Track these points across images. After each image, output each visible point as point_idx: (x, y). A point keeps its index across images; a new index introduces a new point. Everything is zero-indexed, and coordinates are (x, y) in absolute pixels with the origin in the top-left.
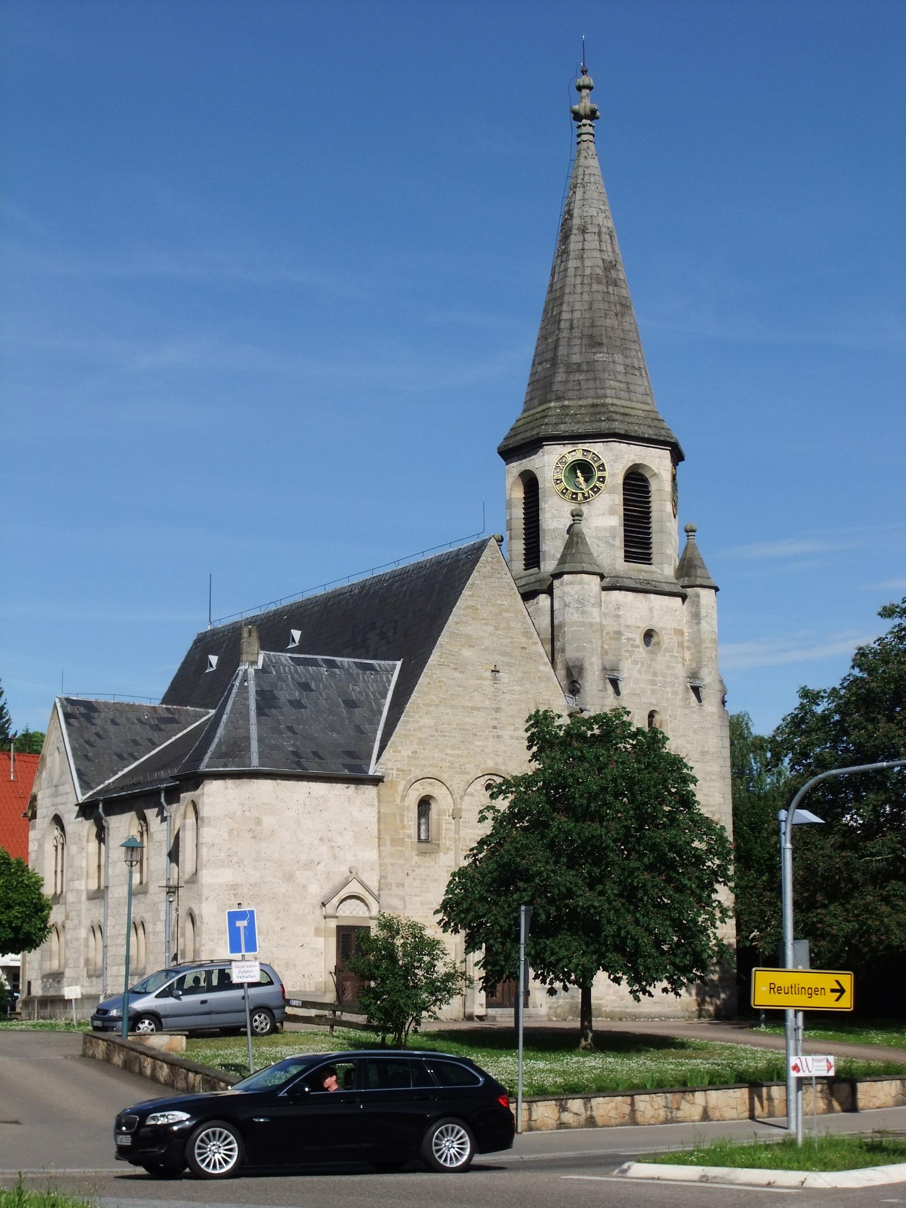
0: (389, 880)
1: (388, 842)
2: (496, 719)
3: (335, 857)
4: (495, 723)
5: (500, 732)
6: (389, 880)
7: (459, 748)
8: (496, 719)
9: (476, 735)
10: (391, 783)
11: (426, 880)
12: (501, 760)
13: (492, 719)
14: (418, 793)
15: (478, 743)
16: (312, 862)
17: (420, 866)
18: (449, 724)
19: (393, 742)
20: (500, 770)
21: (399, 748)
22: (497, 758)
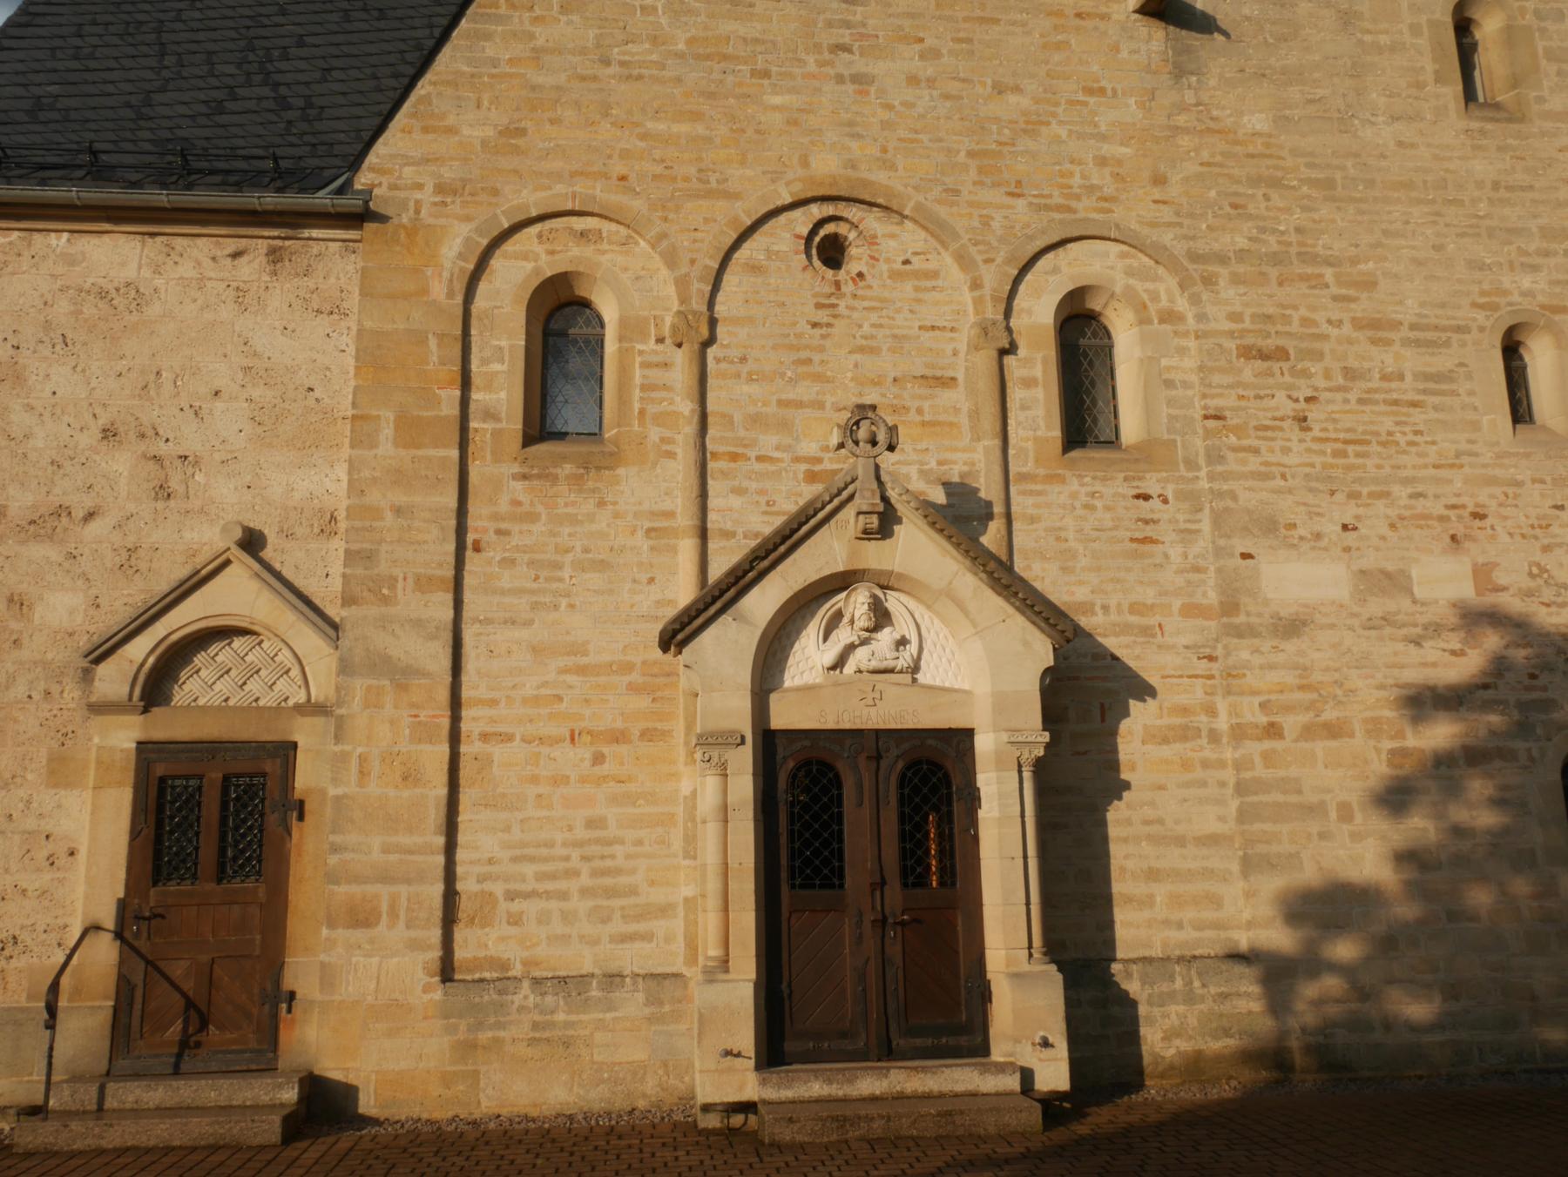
0: (383, 568)
1: (387, 432)
2: (847, 24)
3: (163, 492)
4: (845, 36)
5: (860, 65)
6: (383, 568)
7: (696, 116)
8: (847, 24)
9: (766, 74)
10: (412, 232)
11: (558, 566)
12: (874, 151)
13: (830, 24)
14: (529, 266)
15: (777, 100)
16: (62, 511)
17: (532, 517)
18: (654, 40)
19: (426, 99)
20: (866, 184)
21: (451, 120)
22: (854, 145)
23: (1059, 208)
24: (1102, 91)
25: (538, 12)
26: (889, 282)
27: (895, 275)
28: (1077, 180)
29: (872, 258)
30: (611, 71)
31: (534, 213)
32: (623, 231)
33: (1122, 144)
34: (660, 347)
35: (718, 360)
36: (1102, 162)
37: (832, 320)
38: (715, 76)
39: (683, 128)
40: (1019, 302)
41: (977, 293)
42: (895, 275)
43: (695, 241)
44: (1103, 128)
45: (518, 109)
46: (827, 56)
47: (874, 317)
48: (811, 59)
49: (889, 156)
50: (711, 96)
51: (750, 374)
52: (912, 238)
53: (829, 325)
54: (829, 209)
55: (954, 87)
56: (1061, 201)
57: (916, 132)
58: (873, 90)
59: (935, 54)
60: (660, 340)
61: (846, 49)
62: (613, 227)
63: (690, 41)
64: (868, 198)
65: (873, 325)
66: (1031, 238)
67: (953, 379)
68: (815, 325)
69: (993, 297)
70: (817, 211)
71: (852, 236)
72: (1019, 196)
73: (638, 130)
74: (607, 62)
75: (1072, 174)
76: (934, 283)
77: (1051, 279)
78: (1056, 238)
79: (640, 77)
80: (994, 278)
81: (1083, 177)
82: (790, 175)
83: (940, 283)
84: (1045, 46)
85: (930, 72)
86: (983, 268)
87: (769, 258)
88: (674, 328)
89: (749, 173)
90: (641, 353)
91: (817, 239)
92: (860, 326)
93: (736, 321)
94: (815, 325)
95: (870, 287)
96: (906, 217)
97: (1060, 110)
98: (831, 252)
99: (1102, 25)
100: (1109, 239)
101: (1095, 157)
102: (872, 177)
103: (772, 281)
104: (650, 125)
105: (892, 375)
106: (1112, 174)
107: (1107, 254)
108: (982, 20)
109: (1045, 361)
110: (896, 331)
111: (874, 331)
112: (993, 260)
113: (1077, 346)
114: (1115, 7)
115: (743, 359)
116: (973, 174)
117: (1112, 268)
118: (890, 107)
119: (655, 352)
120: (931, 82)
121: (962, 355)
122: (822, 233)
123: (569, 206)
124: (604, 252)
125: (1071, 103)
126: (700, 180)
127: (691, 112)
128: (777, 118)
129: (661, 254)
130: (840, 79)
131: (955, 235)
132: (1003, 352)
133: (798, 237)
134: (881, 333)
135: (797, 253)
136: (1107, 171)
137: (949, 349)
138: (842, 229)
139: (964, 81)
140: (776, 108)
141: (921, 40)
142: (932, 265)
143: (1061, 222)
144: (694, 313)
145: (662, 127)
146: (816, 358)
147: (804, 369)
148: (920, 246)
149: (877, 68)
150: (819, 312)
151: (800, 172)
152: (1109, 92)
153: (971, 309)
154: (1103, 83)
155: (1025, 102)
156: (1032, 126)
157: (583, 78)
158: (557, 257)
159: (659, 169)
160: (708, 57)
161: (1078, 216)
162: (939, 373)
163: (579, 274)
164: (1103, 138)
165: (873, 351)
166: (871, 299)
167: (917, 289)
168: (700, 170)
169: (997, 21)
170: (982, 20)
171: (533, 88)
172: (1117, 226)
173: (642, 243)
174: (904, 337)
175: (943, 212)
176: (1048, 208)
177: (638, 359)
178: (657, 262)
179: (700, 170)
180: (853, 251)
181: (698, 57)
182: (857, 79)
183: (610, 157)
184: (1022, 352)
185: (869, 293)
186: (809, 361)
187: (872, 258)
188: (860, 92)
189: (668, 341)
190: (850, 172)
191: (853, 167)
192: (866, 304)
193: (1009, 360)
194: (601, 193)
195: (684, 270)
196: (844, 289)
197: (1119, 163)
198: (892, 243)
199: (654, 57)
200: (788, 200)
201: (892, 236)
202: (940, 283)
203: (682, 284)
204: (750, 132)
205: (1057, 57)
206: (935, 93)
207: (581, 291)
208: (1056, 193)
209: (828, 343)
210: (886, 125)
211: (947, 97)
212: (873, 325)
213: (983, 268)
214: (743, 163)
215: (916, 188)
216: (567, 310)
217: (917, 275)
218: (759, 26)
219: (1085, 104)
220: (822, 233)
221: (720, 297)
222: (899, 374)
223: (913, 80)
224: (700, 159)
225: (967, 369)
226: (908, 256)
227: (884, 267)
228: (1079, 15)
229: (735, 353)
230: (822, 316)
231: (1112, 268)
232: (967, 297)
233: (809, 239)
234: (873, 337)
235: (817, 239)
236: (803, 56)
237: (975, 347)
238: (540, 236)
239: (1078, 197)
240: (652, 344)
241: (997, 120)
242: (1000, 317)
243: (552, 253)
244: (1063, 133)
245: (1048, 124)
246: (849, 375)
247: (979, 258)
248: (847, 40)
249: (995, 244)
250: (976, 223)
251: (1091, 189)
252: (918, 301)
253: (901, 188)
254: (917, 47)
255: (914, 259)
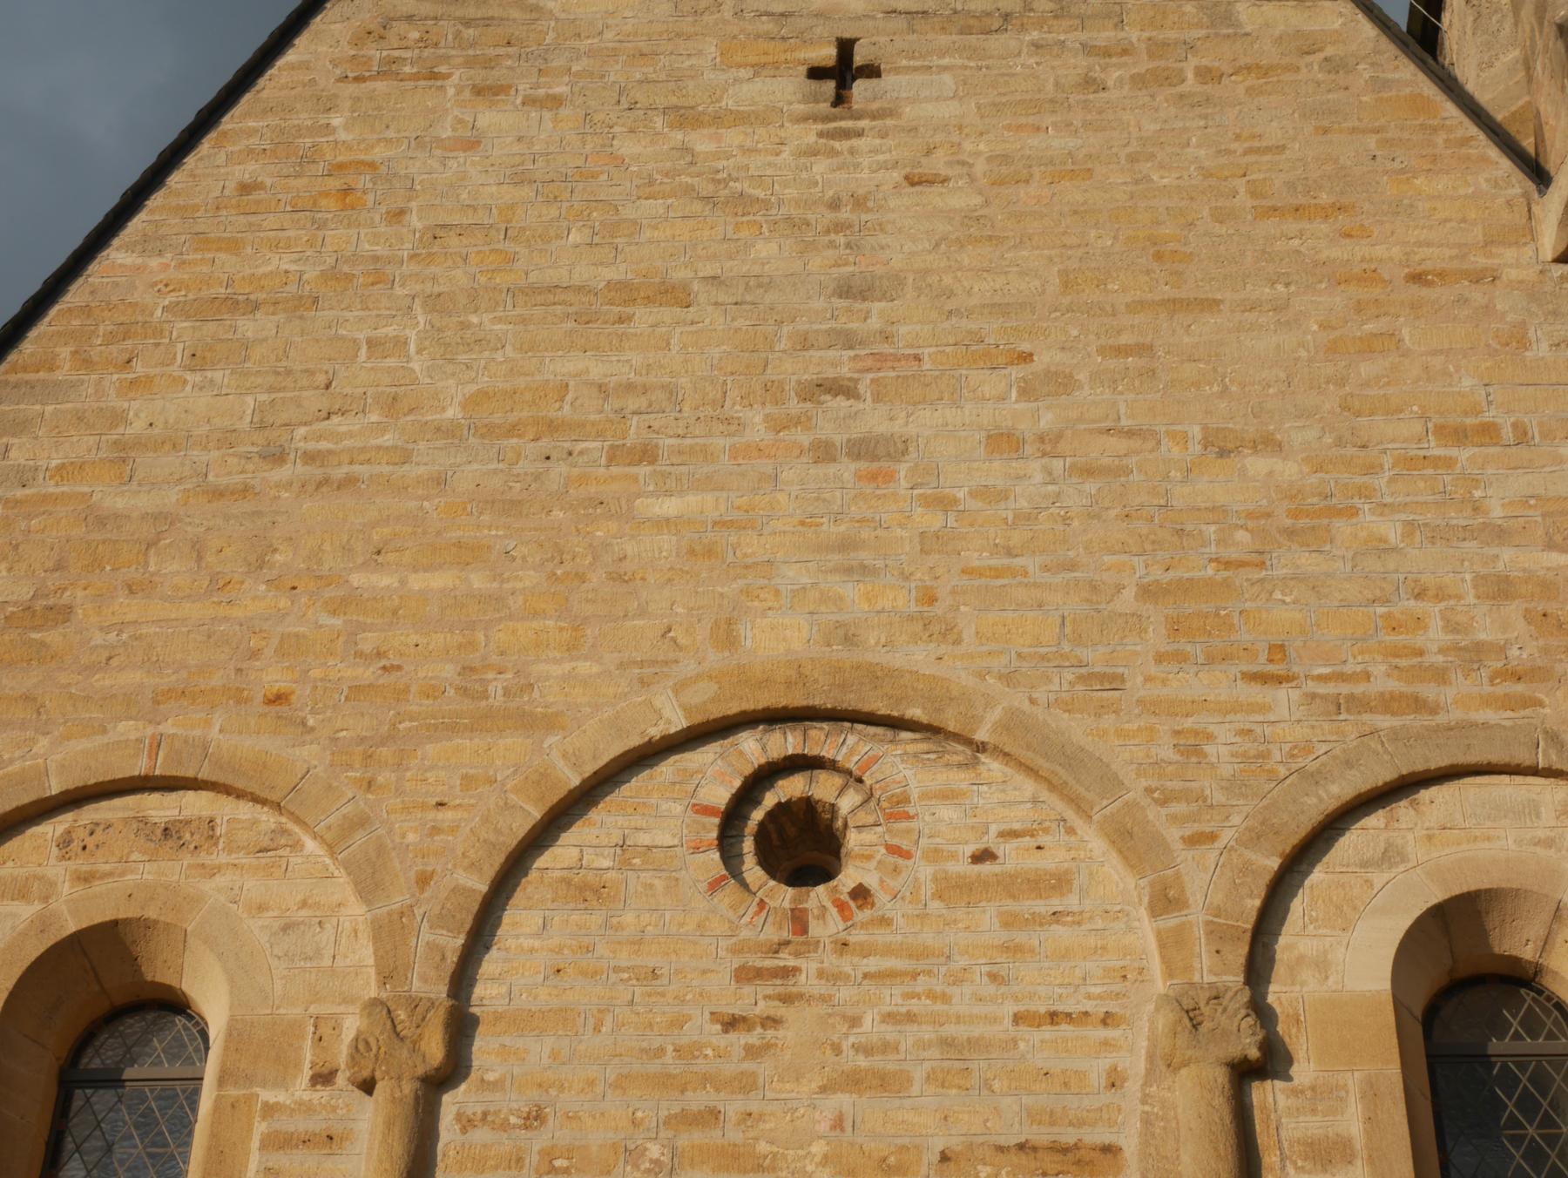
2: (848, 340)
4: (841, 363)
5: (874, 419)
7: (467, 554)
8: (848, 340)
9: (647, 454)
12: (901, 600)
14: (27, 911)
15: (669, 507)
18: (392, 405)
20: (876, 676)
22: (851, 591)
23: (1388, 703)
24: (1488, 432)
25: (139, 368)
26: (935, 905)
27: (950, 889)
28: (1435, 636)
29: (893, 850)
30: (284, 473)
31: (55, 787)
32: (267, 819)
33: (1550, 546)
34: (322, 1094)
35: (466, 1123)
36: (1499, 589)
37: (779, 1010)
38: (523, 467)
39: (440, 580)
40: (1291, 942)
41: (1170, 921)
42: (950, 889)
43: (436, 830)
44: (1497, 512)
45: (59, 566)
46: (794, 406)
47: (892, 997)
48: (756, 417)
49: (938, 609)
50: (512, 507)
51: (548, 1155)
52: (1000, 797)
53: (771, 1022)
54: (785, 742)
55: (1105, 450)
56: (1394, 685)
57: (1009, 553)
58: (903, 469)
59: (1061, 382)
60: (323, 1078)
61: (845, 389)
62: (245, 810)
63: (471, 403)
64: (882, 709)
65: (889, 1018)
66: (1315, 778)
67: (1109, 1150)
68: (732, 1023)
69: (1213, 931)
70: (754, 748)
71: (847, 803)
72: (1279, 680)
73: (329, 593)
74: (277, 457)
75: (1420, 622)
76: (1056, 904)
77: (1379, 878)
78: (1382, 774)
79: (349, 482)
80: (1221, 885)
81: (1451, 626)
82: (688, 667)
83: (1072, 902)
84: (1333, 349)
85: (1047, 421)
86: (1186, 859)
87: (624, 864)
88: (360, 1045)
89: (585, 667)
90: (269, 1110)
91: (758, 815)
92: (855, 1022)
93: (524, 1022)
94: (732, 1023)
95: (885, 921)
96: (981, 748)
97: (1381, 481)
98: (802, 848)
99: (1477, 296)
100: (1534, 771)
101: (1479, 580)
102: (897, 660)
103: (629, 918)
104: (357, 579)
105: (939, 1144)
106: (1528, 616)
107: (1533, 810)
108: (1175, 306)
109: (1371, 1093)
110: (950, 1030)
111: (890, 1032)
112: (1212, 837)
113: (1485, 1060)
114: (1510, 254)
115: (535, 1118)
116: (1156, 637)
117: (1549, 843)
118: (944, 503)
119: (307, 1108)
120: (1048, 444)
121: (1133, 1087)
122: (770, 800)
123: (140, 767)
124: (213, 872)
125: (1409, 463)
126: (464, 691)
127: (459, 545)
128: (667, 541)
129: (347, 866)
130: (824, 452)
131: (1111, 783)
132: (1245, 1073)
133: (706, 810)
134: (909, 1036)
135: (696, 849)
136: (1514, 610)
137: (1096, 1070)
138: (823, 787)
139: (1130, 433)
140: (664, 523)
141: (1026, 357)
142: (1049, 861)
143: (1395, 736)
144: (414, 1004)
145: (385, 581)
146: (733, 1107)
147: (697, 1137)
148: (1019, 817)
149: (923, 422)
150: (747, 990)
151: (715, 658)
152: (1508, 434)
153: (1156, 966)
154: (1489, 415)
155: (1289, 470)
156: (1310, 519)
157: (218, 494)
158: (99, 887)
159: (367, 674)
160: (513, 430)
161: (1441, 719)
162: (1069, 1136)
163: (147, 925)
164: (1500, 534)
165: (888, 1083)
166: (888, 951)
167: (1010, 921)
168: (467, 670)
169: (1212, 305)
170: (1175, 306)
171: (102, 522)
172: (1554, 738)
173: (310, 845)
174: (972, 1043)
175: (1077, 729)
176: (1359, 704)
177: (260, 1128)
178: (342, 887)
179: (467, 670)
180: (853, 840)
181: (490, 431)
182: (862, 449)
183: (255, 654)
184: (1303, 1071)
185: (881, 936)
186: (713, 1116)
187: (893, 850)
188: (873, 477)
189: (341, 1080)
190: (839, 652)
191: (849, 640)
192: (873, 964)
193: (1264, 1094)
194: (226, 737)
195: (399, 900)
196: (815, 929)
197: (1547, 588)
198: (947, 813)
199: (388, 439)
200: (676, 721)
201: (948, 796)
202: (1072, 902)
203: (390, 935)
204: (596, 578)
205: (1366, 369)
206: (1057, 465)
207: (159, 972)
208: (1379, 669)
209: (763, 1068)
210: (929, 542)
211: (1089, 472)
212: (889, 1018)
213: (1186, 859)
214: (572, 648)
215: (1008, 678)
216: (133, 1026)
217: (1012, 886)
218: (637, 359)
219: (1449, 463)
220: (770, 800)
221: (490, 965)
222: (955, 1143)
223: (1003, 442)
224: (471, 645)
225: (1147, 1121)
226: (990, 841)
227: (925, 871)
228: (1417, 278)
229: (513, 1103)
230: (752, 1000)
231: (1549, 843)
232: (1146, 931)
233: (733, 817)
234: (886, 1047)
235: (758, 815)
236: (738, 411)
237: (1166, 1063)
238: (65, 842)
239: (1440, 676)
240: (300, 1089)
241: (1218, 513)
242: (1234, 979)
243: (86, 878)
244: (1391, 530)
245: (1353, 512)
246: (818, 1148)
247: (1174, 834)
248: (845, 371)
249: (1219, 797)
250: (1168, 753)
251: (1476, 653)
252: (1013, 950)
253: (966, 680)
254: (1016, 372)
255: (1004, 849)
